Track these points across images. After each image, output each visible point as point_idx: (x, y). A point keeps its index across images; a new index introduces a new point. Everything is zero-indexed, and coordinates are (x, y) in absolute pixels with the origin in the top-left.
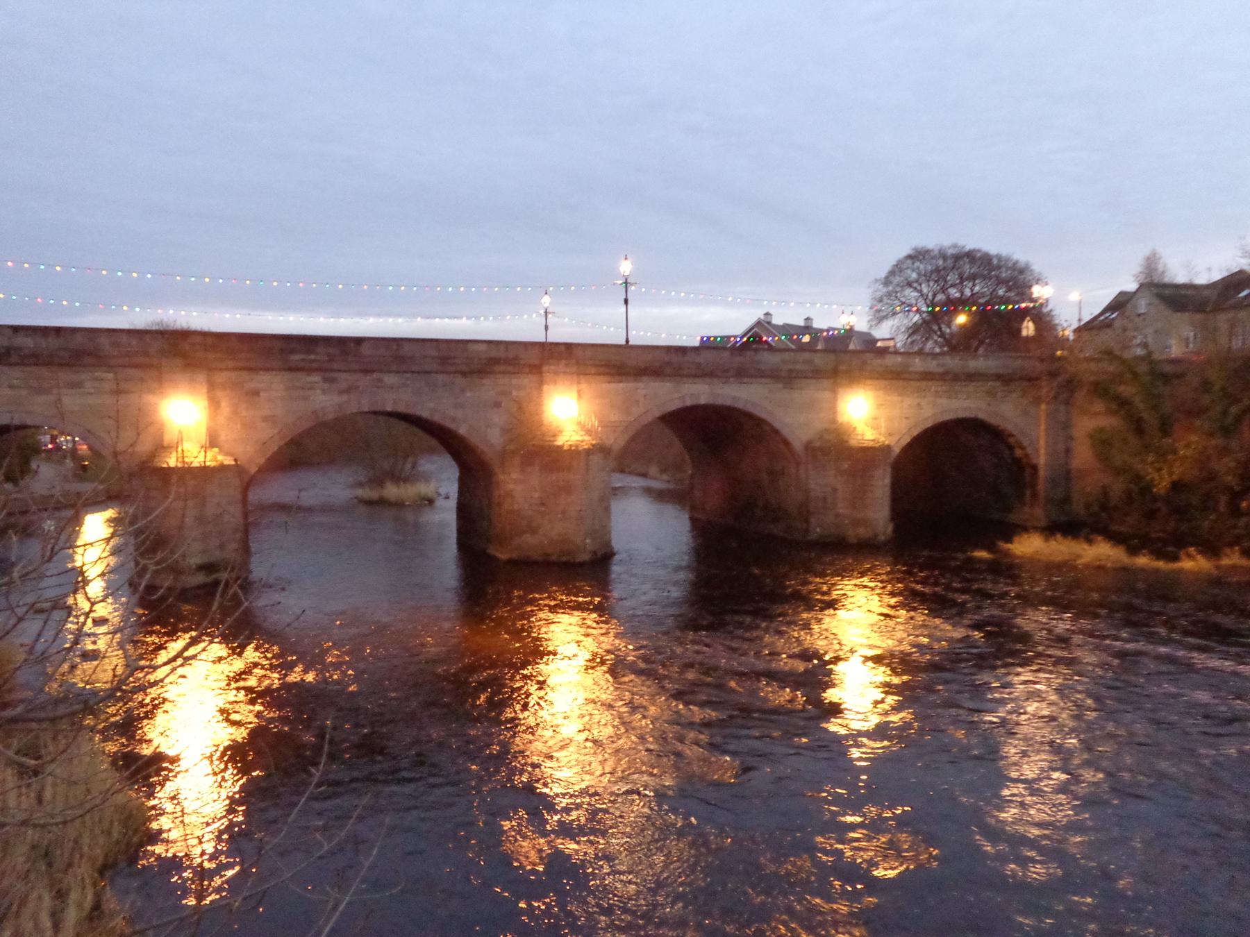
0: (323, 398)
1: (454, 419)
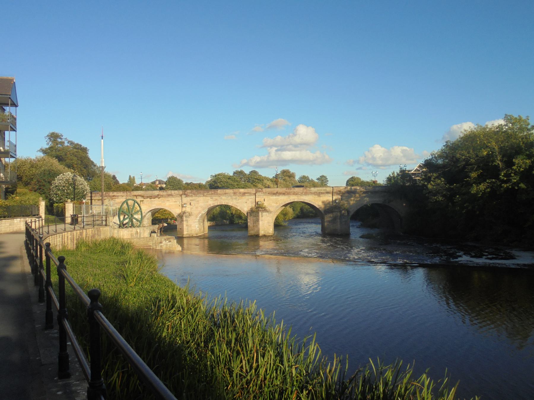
1: (237, 206)
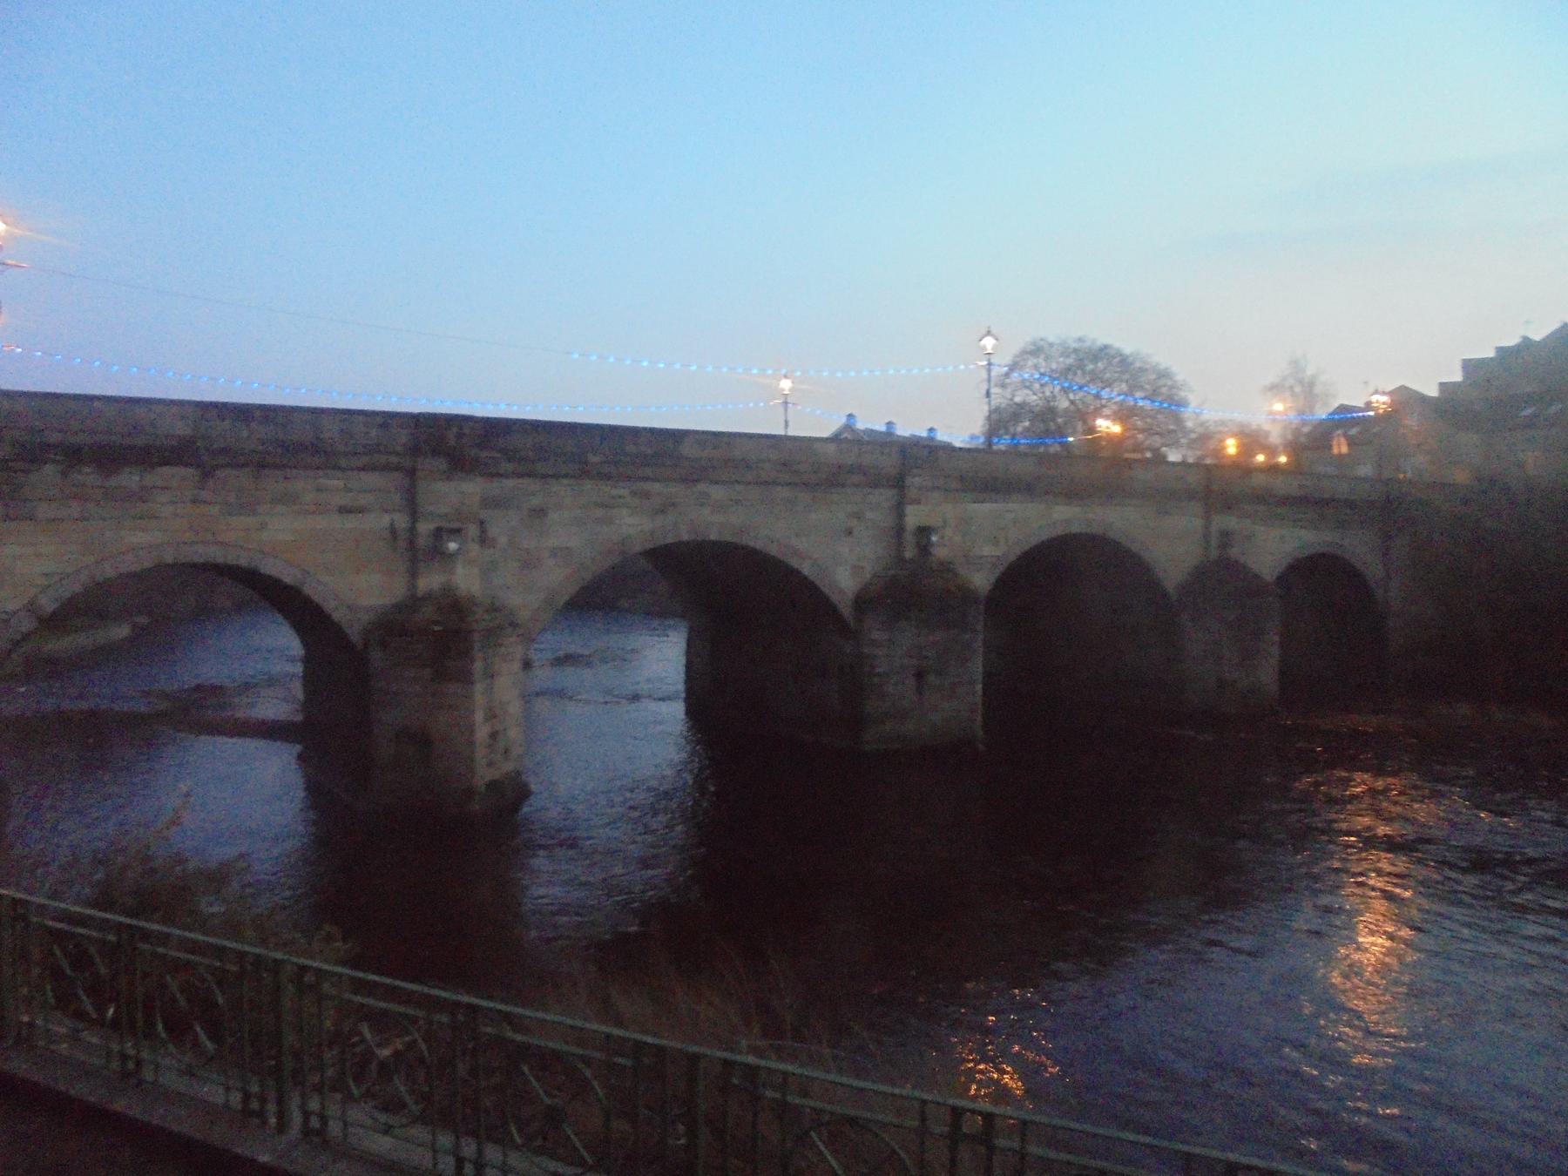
0: (630, 520)
